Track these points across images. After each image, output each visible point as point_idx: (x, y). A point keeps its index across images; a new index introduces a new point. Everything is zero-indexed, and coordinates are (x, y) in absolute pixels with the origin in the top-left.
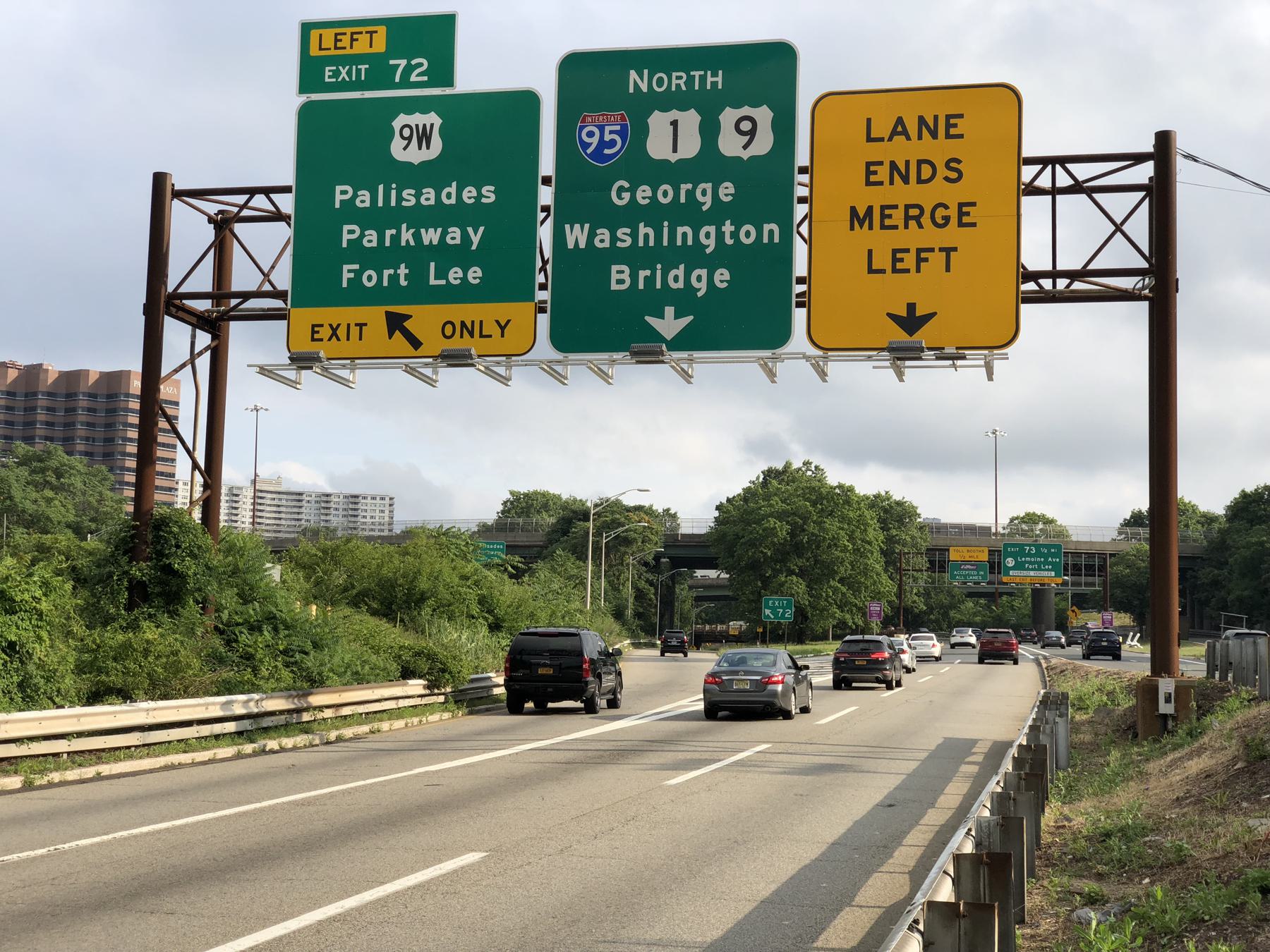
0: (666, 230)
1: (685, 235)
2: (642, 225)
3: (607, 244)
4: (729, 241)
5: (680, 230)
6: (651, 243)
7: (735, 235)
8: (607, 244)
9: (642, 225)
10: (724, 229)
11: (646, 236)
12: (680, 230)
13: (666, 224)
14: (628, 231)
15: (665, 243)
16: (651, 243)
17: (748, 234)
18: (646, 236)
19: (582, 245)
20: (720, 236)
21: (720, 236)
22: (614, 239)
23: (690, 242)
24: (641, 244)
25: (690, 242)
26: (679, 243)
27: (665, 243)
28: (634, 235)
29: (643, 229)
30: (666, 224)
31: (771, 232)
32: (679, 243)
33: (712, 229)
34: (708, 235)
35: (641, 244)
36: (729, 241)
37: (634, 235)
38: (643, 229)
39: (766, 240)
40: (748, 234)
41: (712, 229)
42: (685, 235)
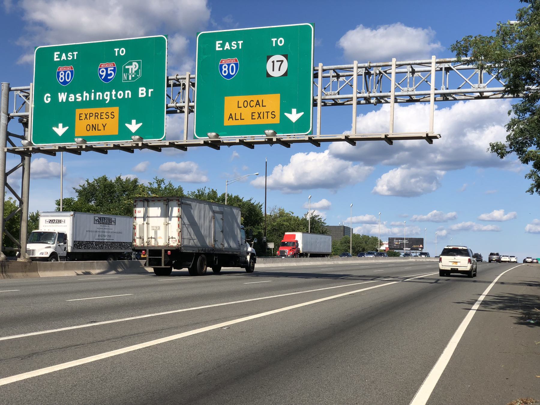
1: (99, 95)
3: (73, 100)
5: (98, 94)
8: (73, 100)
11: (86, 96)
12: (98, 94)
15: (93, 99)
18: (86, 96)
19: (64, 101)
24: (84, 99)
26: (97, 99)
27: (93, 99)
31: (128, 93)
32: (97, 99)
35: (84, 99)
37: (82, 96)
39: (126, 97)
42: (99, 95)
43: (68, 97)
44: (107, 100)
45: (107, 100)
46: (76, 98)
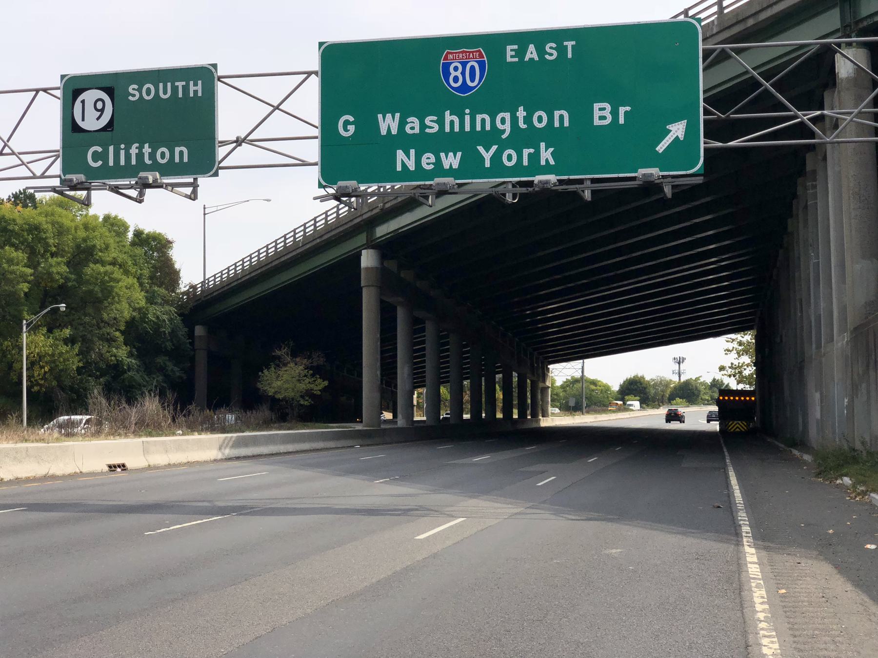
1: (483, 121)
2: (447, 113)
4: (522, 125)
5: (479, 118)
7: (528, 120)
9: (447, 113)
11: (452, 122)
14: (435, 118)
16: (457, 129)
17: (540, 119)
18: (452, 122)
20: (514, 120)
21: (514, 120)
22: (423, 126)
23: (488, 128)
25: (488, 128)
26: (478, 128)
29: (448, 117)
33: (507, 116)
34: (503, 121)
35: (447, 129)
36: (522, 125)
38: (448, 117)
41: (507, 116)
42: (483, 121)
44: (504, 131)
45: (504, 131)
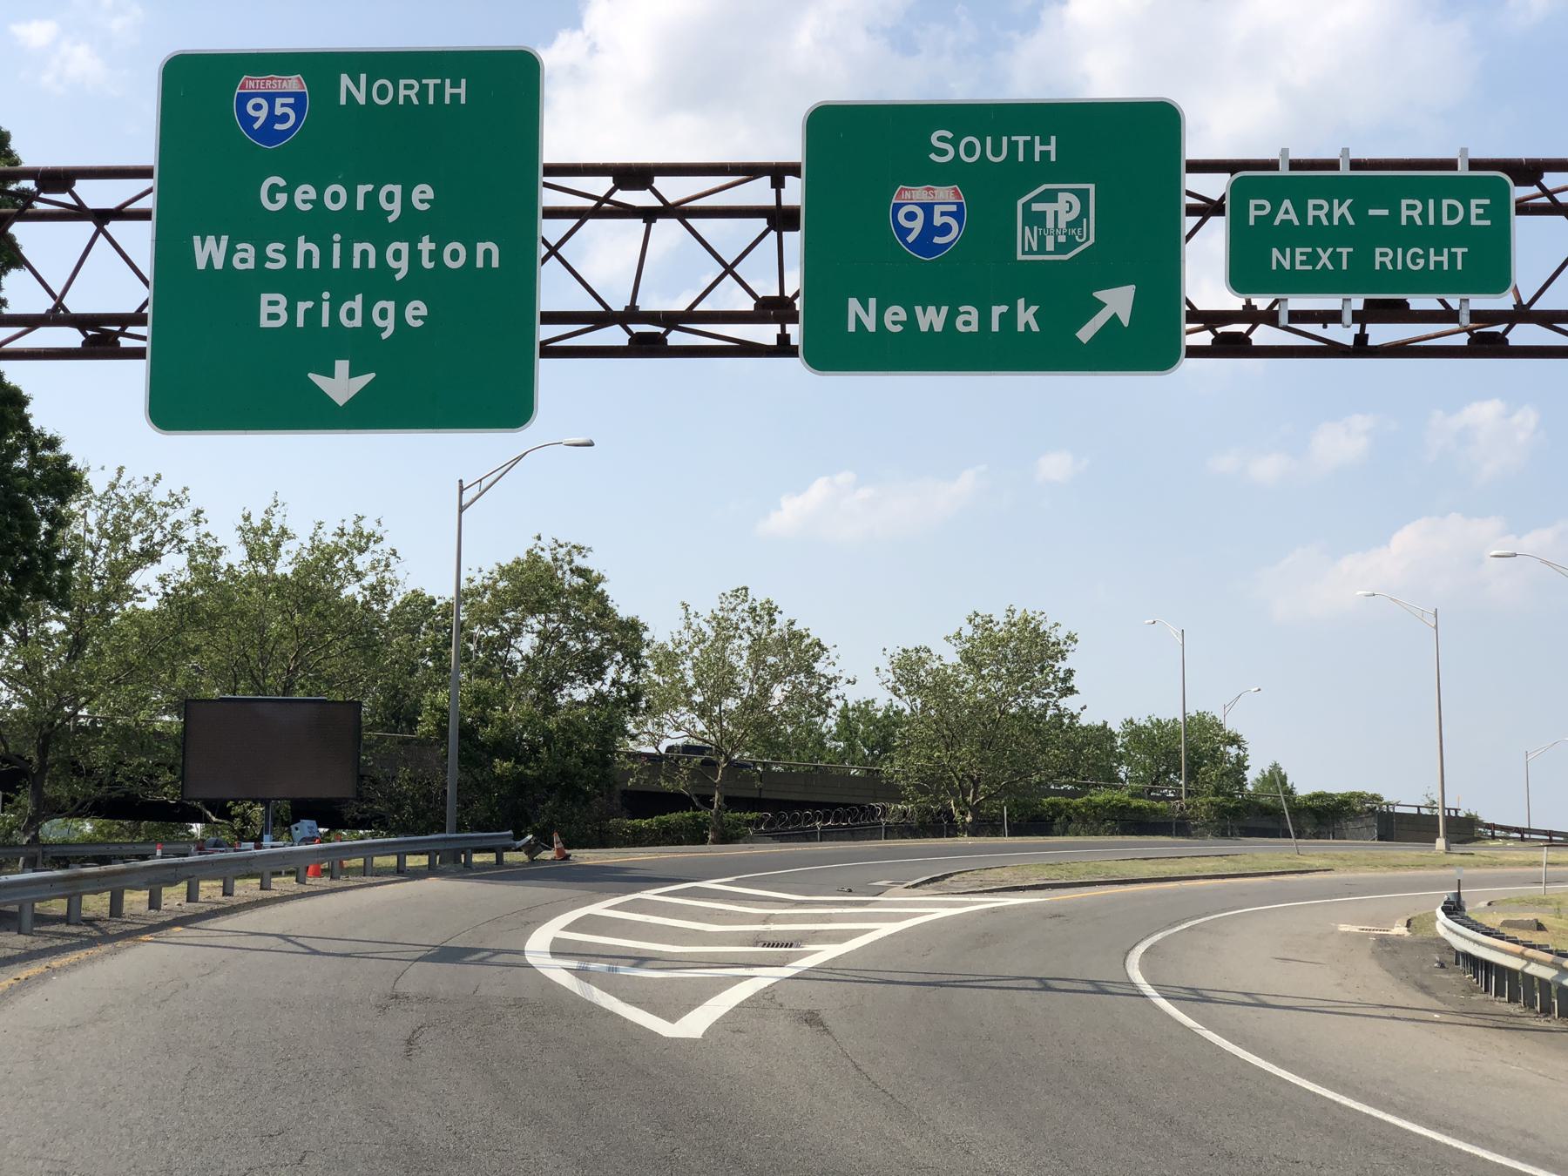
0: (337, 248)
1: (364, 254)
2: (301, 239)
3: (251, 265)
4: (427, 264)
5: (358, 248)
6: (316, 264)
7: (436, 255)
8: (251, 265)
9: (301, 239)
10: (420, 246)
11: (308, 254)
12: (358, 248)
13: (337, 237)
14: (281, 247)
15: (336, 264)
16: (316, 264)
17: (455, 255)
18: (308, 254)
20: (415, 255)
21: (415, 255)
23: (372, 264)
24: (300, 265)
25: (372, 264)
26: (356, 264)
27: (336, 264)
28: (290, 253)
29: (302, 245)
30: (337, 237)
31: (488, 253)
32: (356, 264)
33: (404, 247)
34: (397, 255)
35: (300, 265)
36: (427, 264)
37: (290, 253)
38: (302, 245)
39: (480, 264)
40: (455, 255)
41: (404, 247)
42: (364, 254)
43: (231, 251)
46: (261, 258)
